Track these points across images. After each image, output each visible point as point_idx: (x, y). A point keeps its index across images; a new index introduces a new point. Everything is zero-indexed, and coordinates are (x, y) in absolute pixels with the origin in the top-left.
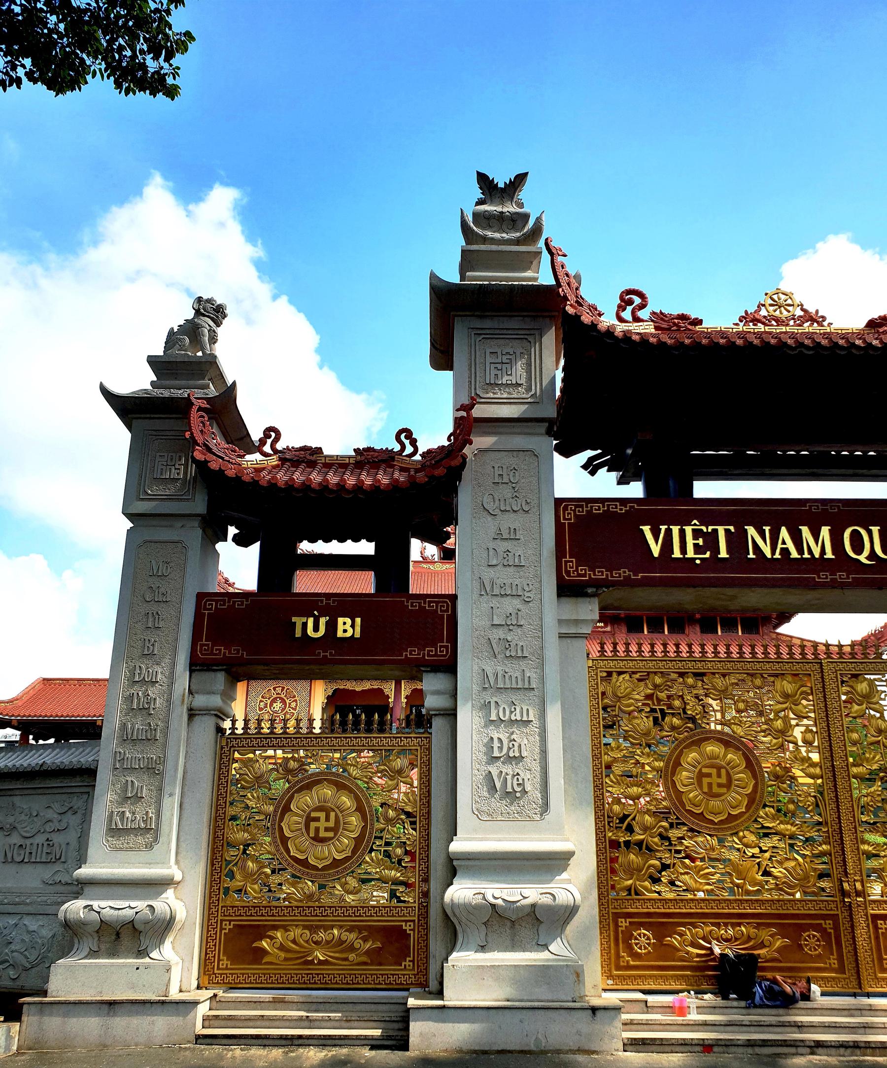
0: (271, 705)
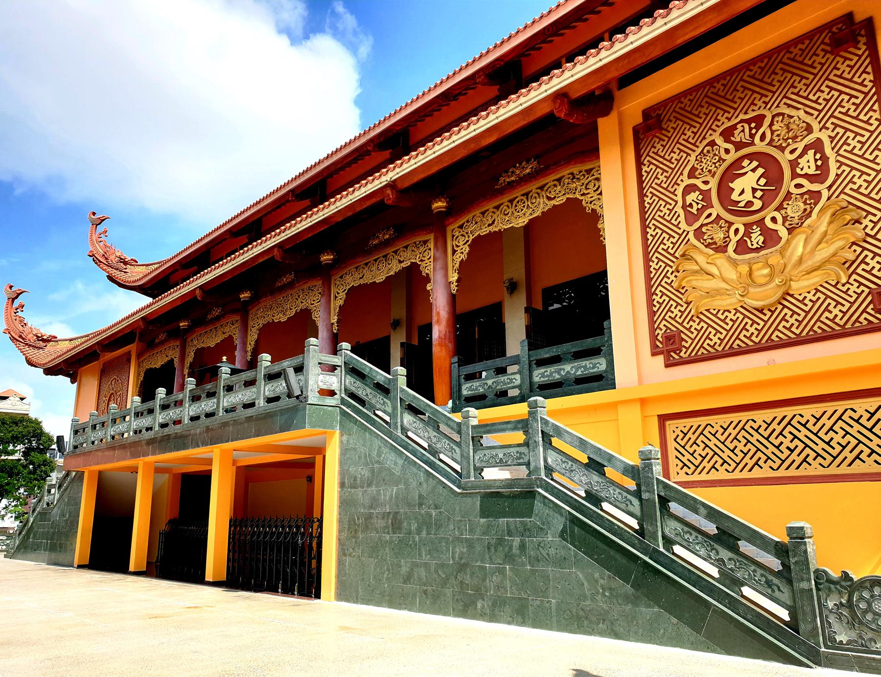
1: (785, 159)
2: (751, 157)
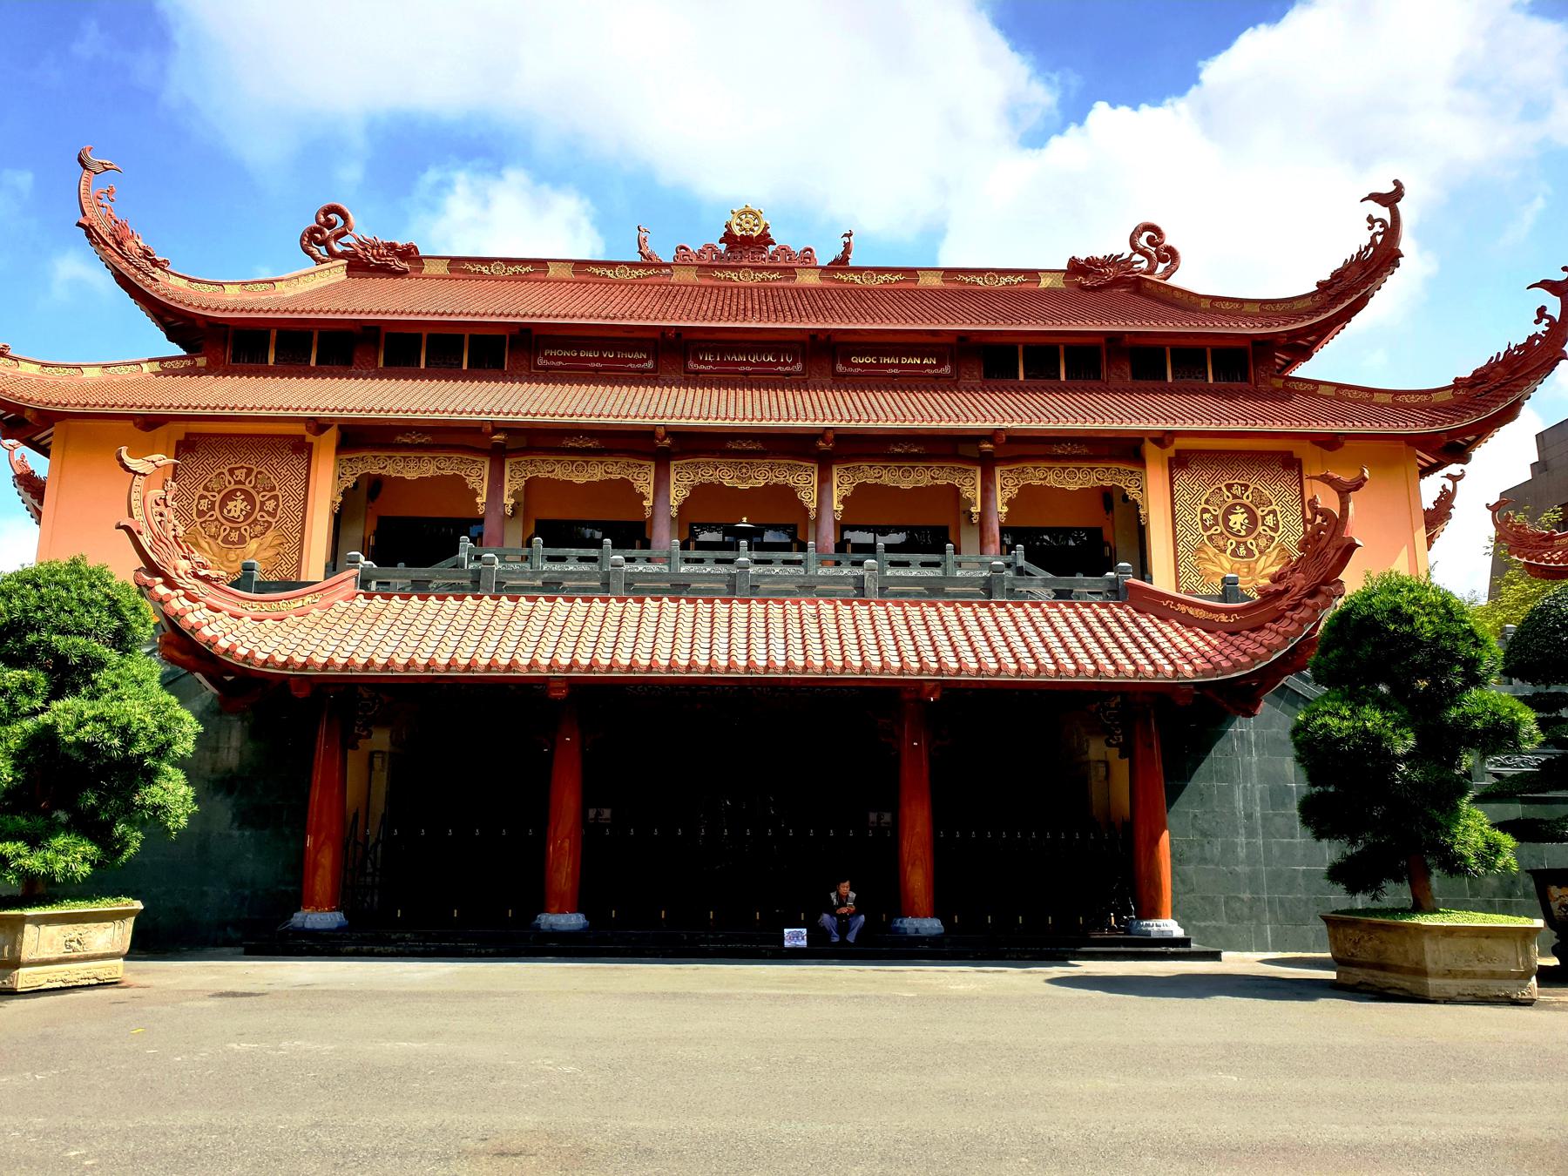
1: (1259, 513)
2: (1242, 505)
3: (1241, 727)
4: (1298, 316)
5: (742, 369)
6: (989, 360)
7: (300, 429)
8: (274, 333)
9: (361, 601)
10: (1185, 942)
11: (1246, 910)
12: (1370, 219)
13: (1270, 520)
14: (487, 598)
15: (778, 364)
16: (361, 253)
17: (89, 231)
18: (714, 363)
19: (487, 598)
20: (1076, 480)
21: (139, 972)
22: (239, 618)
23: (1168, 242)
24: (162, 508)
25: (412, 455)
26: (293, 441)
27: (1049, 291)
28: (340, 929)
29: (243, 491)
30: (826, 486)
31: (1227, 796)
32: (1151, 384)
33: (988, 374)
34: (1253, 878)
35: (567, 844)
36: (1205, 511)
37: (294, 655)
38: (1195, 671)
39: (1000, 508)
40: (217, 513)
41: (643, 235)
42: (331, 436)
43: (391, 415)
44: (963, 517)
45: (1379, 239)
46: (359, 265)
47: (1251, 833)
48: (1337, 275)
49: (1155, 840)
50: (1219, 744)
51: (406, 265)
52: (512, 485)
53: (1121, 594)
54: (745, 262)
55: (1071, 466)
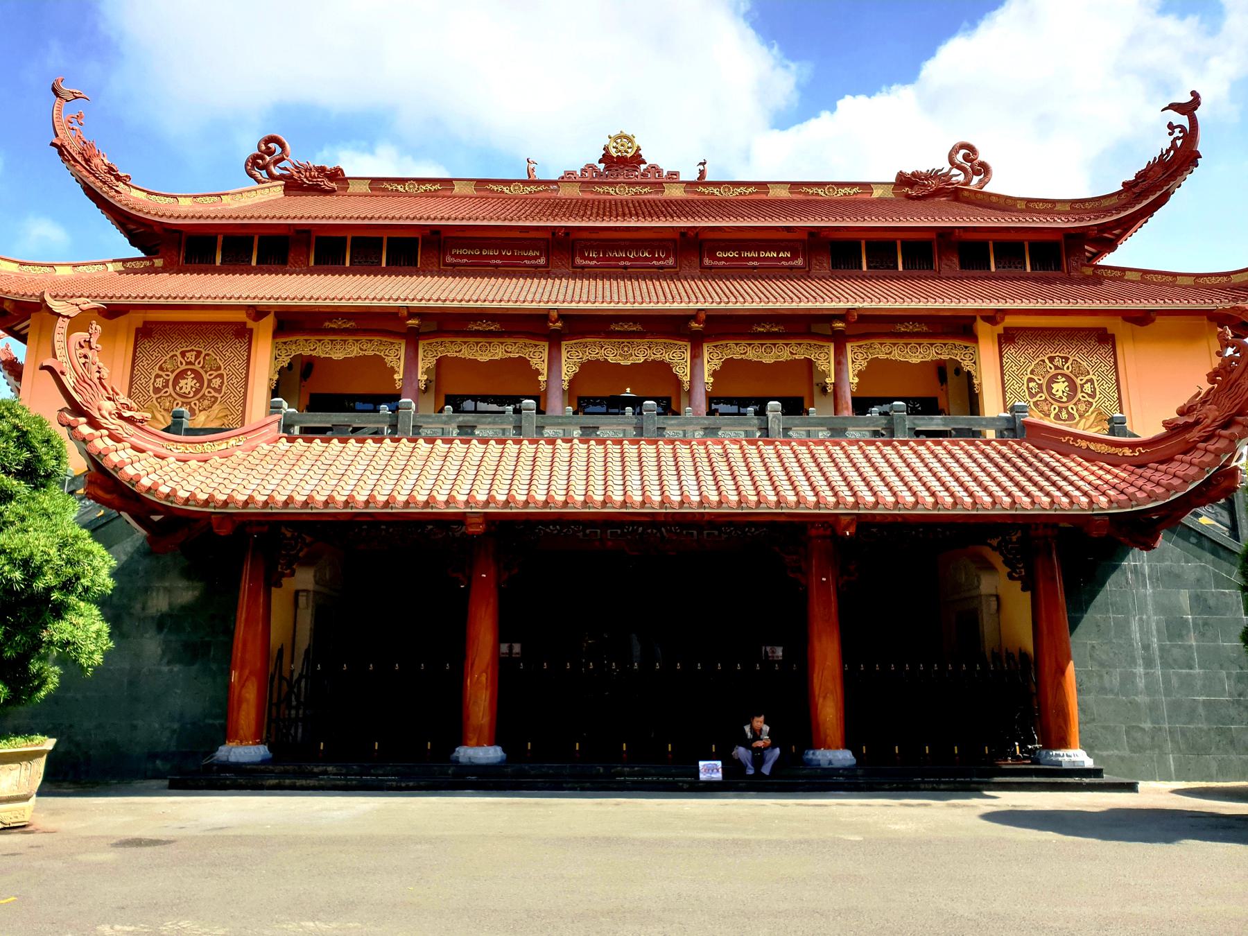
0: (176, 382)
1: (1078, 382)
3: (1137, 560)
4: (1108, 211)
5: (622, 263)
6: (838, 252)
7: (241, 316)
8: (220, 240)
9: (283, 445)
10: (1097, 773)
11: (1148, 740)
12: (1170, 126)
13: (1088, 388)
14: (404, 440)
15: (653, 258)
16: (296, 176)
17: (61, 149)
18: (598, 259)
19: (404, 440)
20: (918, 354)
21: (54, 812)
22: (163, 458)
23: (981, 158)
24: (86, 351)
25: (338, 338)
26: (235, 328)
27: (881, 201)
28: (264, 762)
29: (193, 371)
30: (698, 361)
31: (1123, 628)
32: (976, 272)
33: (835, 265)
34: (1153, 708)
35: (484, 678)
36: (1030, 380)
37: (216, 493)
38: (1110, 502)
39: (852, 379)
40: (170, 390)
41: (532, 166)
42: (269, 322)
43: (320, 302)
44: (816, 390)
45: (1179, 143)
46: (293, 186)
47: (1149, 663)
48: (1141, 176)
49: (1061, 671)
50: (1114, 577)
51: (334, 185)
52: (425, 363)
53: (1018, 431)
54: (621, 179)
55: (913, 341)
